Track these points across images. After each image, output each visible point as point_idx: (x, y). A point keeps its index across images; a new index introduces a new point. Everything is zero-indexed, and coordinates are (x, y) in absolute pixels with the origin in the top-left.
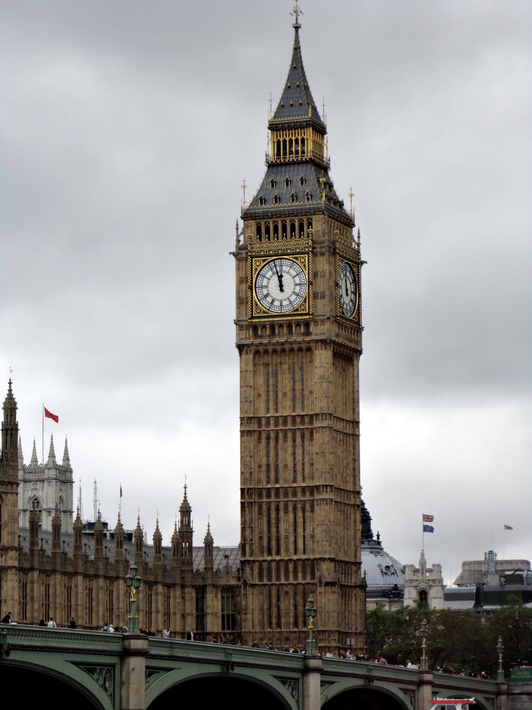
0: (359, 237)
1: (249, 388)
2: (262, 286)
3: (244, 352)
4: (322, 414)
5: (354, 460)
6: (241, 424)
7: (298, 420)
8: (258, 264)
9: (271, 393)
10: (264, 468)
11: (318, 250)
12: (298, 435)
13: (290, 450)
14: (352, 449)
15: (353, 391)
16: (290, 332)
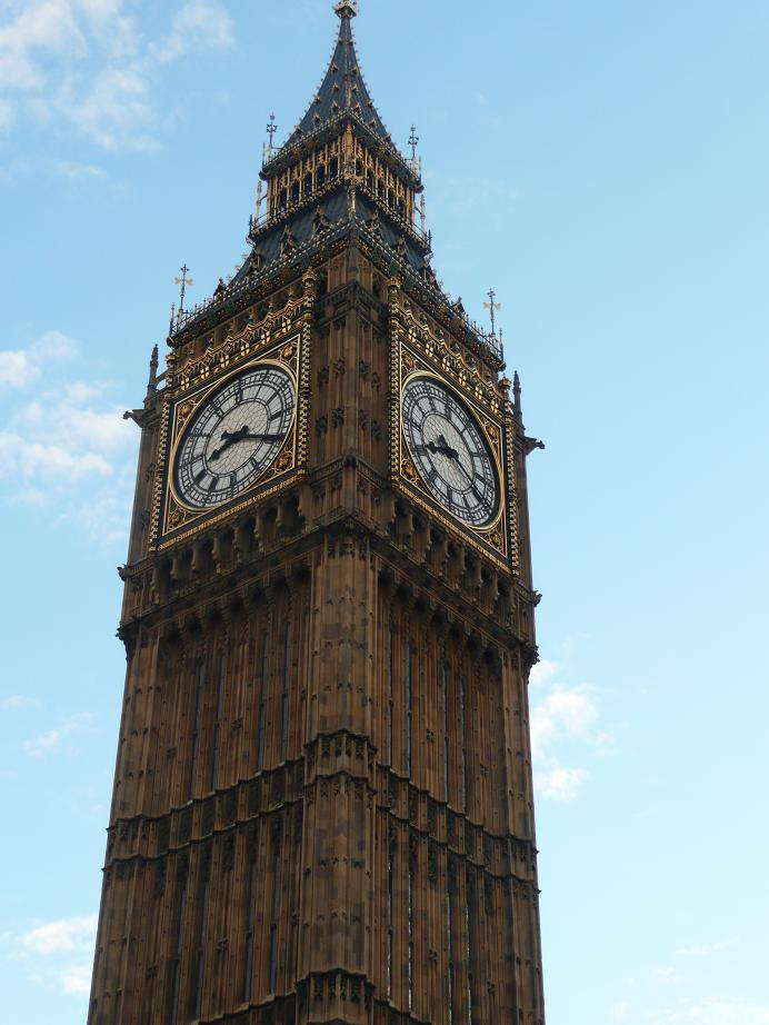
0: (517, 391)
1: (140, 737)
2: (193, 458)
3: (138, 643)
4: (326, 738)
5: (510, 958)
6: (110, 848)
7: (266, 789)
8: (185, 410)
9: (201, 735)
10: (162, 975)
11: (329, 311)
12: (264, 834)
13: (237, 890)
14: (500, 922)
15: (502, 750)
16: (254, 544)
